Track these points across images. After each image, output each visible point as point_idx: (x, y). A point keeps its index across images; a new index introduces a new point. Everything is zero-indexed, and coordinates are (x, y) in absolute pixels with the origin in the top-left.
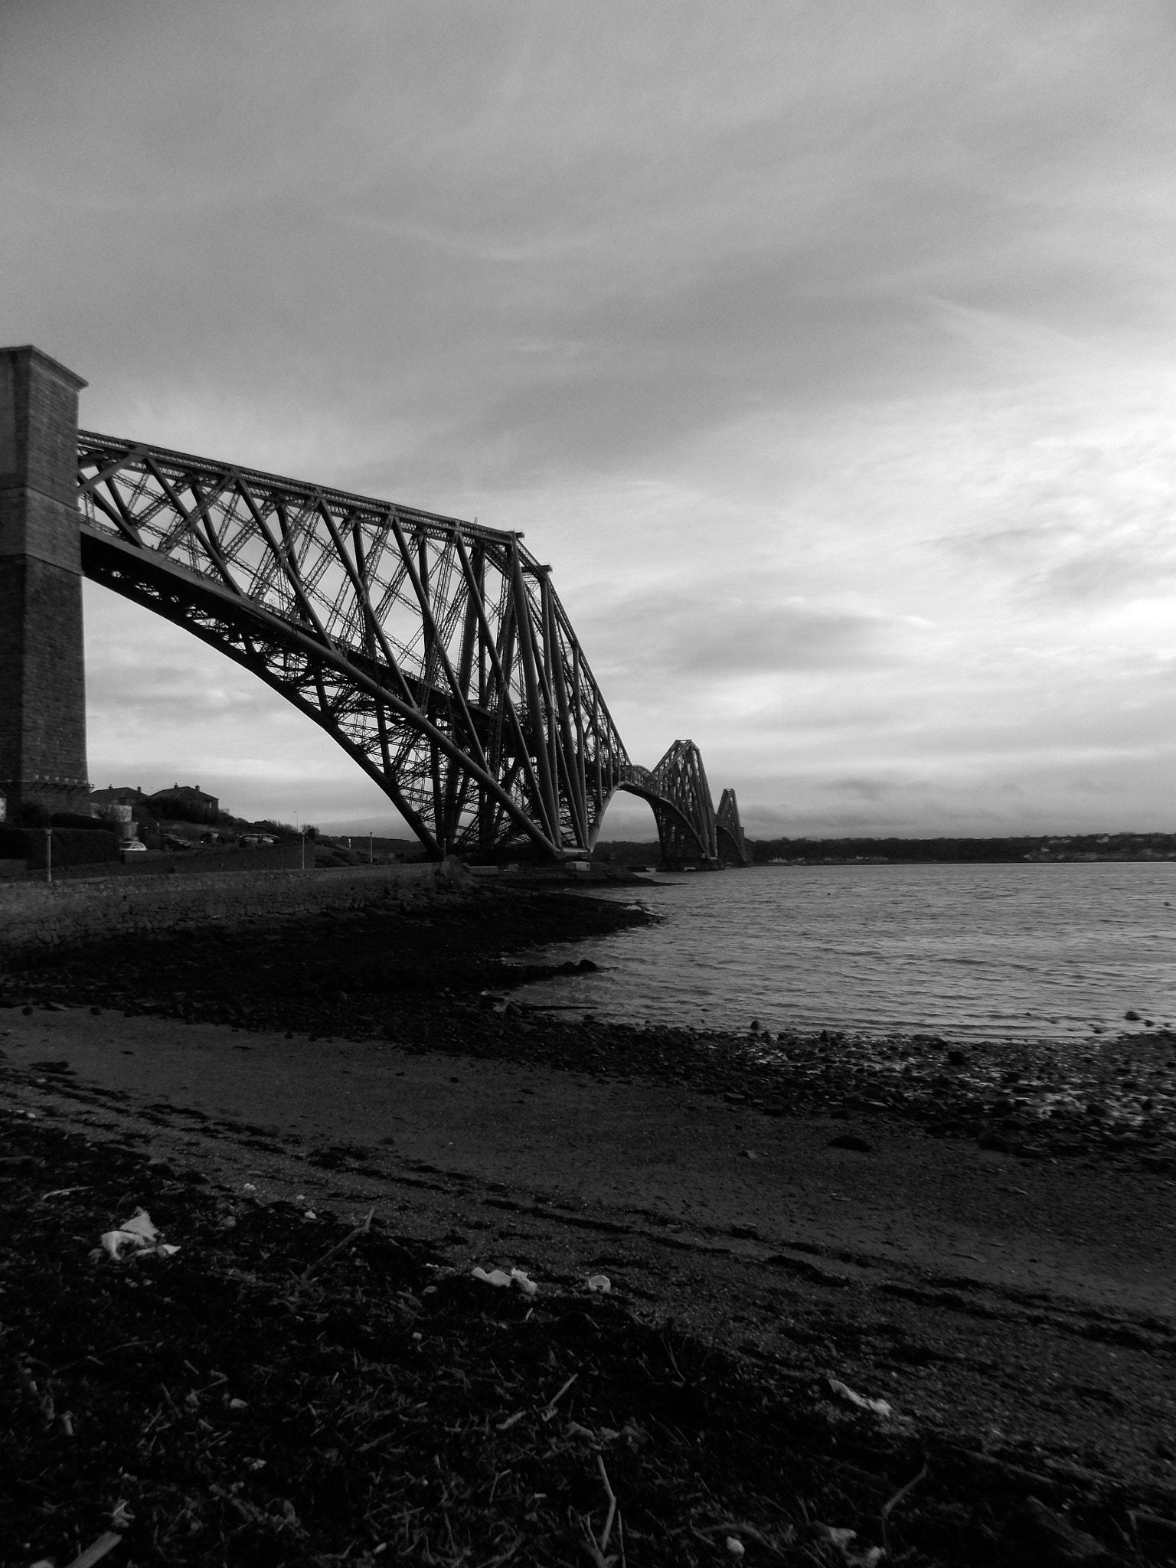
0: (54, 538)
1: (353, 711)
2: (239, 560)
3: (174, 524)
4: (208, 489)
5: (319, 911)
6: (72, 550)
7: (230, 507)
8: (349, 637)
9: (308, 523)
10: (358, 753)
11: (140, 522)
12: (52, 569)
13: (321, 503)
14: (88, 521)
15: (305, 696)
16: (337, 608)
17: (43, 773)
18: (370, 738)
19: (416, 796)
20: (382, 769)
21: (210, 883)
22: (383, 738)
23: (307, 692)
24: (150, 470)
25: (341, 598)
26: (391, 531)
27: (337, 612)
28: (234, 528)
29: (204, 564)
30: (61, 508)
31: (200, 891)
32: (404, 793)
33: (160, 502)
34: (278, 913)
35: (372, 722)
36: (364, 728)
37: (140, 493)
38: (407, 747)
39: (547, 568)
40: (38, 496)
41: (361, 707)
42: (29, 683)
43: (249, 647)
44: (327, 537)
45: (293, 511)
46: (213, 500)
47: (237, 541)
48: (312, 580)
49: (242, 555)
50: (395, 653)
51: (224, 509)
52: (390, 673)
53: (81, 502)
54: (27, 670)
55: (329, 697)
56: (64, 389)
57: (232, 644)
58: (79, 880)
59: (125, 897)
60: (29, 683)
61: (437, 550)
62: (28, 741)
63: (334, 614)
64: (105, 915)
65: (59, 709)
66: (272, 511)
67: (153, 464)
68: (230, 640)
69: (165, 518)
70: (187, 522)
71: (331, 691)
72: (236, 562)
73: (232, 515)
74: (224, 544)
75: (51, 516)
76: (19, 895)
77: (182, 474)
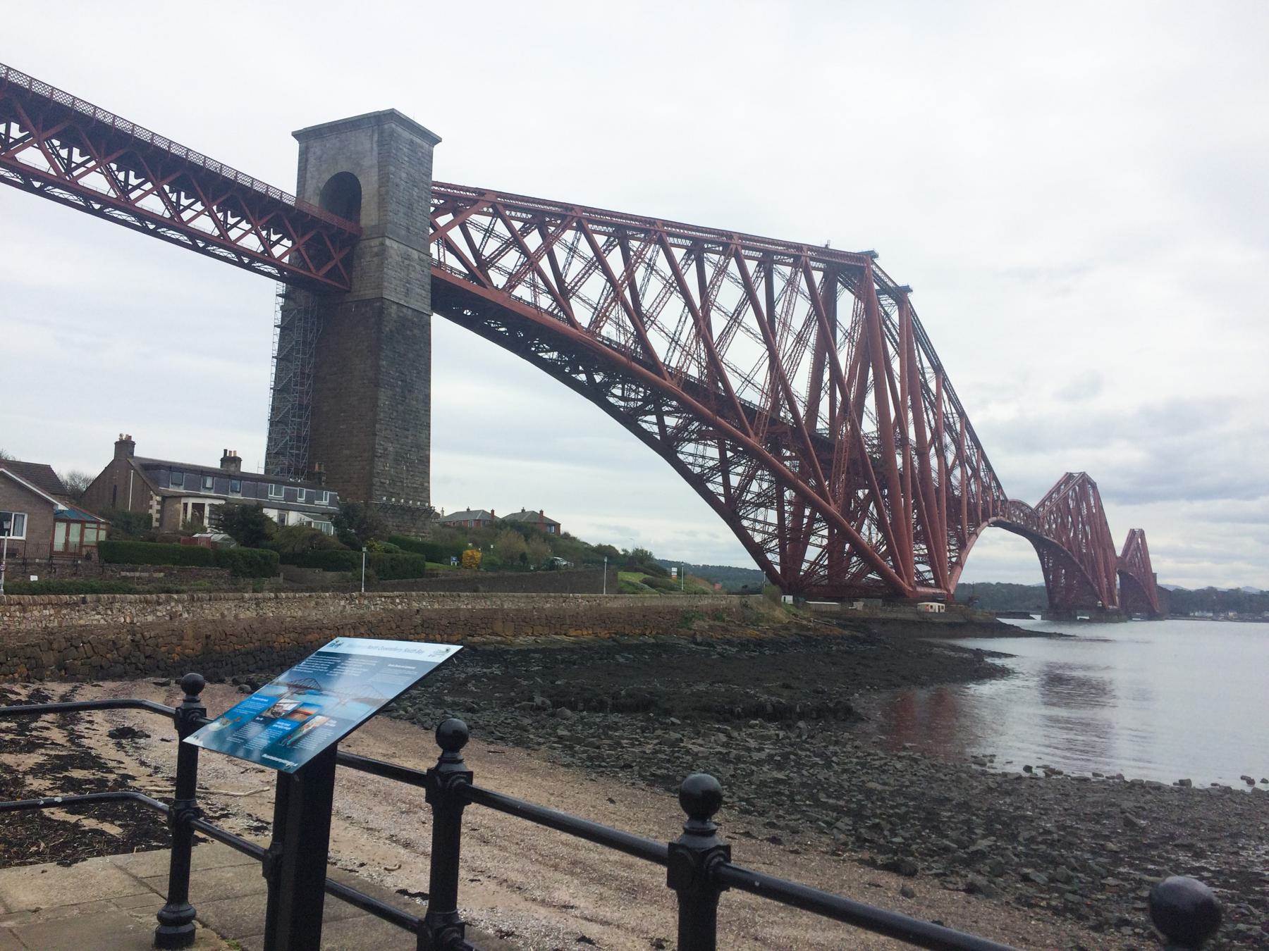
1: (690, 441)
3: (519, 263)
4: (553, 229)
5: (608, 635)
8: (685, 367)
9: (648, 256)
10: (698, 482)
12: (405, 310)
13: (661, 236)
14: (440, 265)
15: (644, 425)
16: (676, 338)
17: (391, 495)
18: (709, 468)
19: (758, 526)
20: (722, 499)
21: (499, 603)
22: (724, 467)
23: (646, 422)
24: (497, 214)
25: (680, 328)
26: (733, 260)
27: (676, 343)
28: (577, 266)
29: (545, 302)
30: (415, 255)
31: (489, 609)
32: (745, 523)
33: (507, 246)
34: (565, 634)
35: (713, 452)
36: (703, 457)
37: (489, 237)
38: (748, 478)
39: (907, 290)
40: (395, 245)
41: (701, 437)
42: (382, 414)
44: (668, 272)
45: (634, 244)
46: (557, 238)
47: (580, 276)
49: (584, 291)
50: (735, 383)
51: (566, 246)
52: (727, 403)
53: (433, 248)
54: (380, 403)
55: (668, 426)
56: (422, 147)
57: (574, 376)
58: (376, 594)
59: (418, 611)
60: (382, 414)
61: (783, 276)
62: (379, 466)
63: (674, 344)
64: (398, 627)
65: (407, 438)
66: (615, 246)
67: (500, 208)
68: (571, 372)
69: (512, 260)
70: (531, 262)
71: (671, 421)
72: (580, 298)
73: (575, 252)
74: (568, 280)
76: (317, 604)
77: (530, 216)
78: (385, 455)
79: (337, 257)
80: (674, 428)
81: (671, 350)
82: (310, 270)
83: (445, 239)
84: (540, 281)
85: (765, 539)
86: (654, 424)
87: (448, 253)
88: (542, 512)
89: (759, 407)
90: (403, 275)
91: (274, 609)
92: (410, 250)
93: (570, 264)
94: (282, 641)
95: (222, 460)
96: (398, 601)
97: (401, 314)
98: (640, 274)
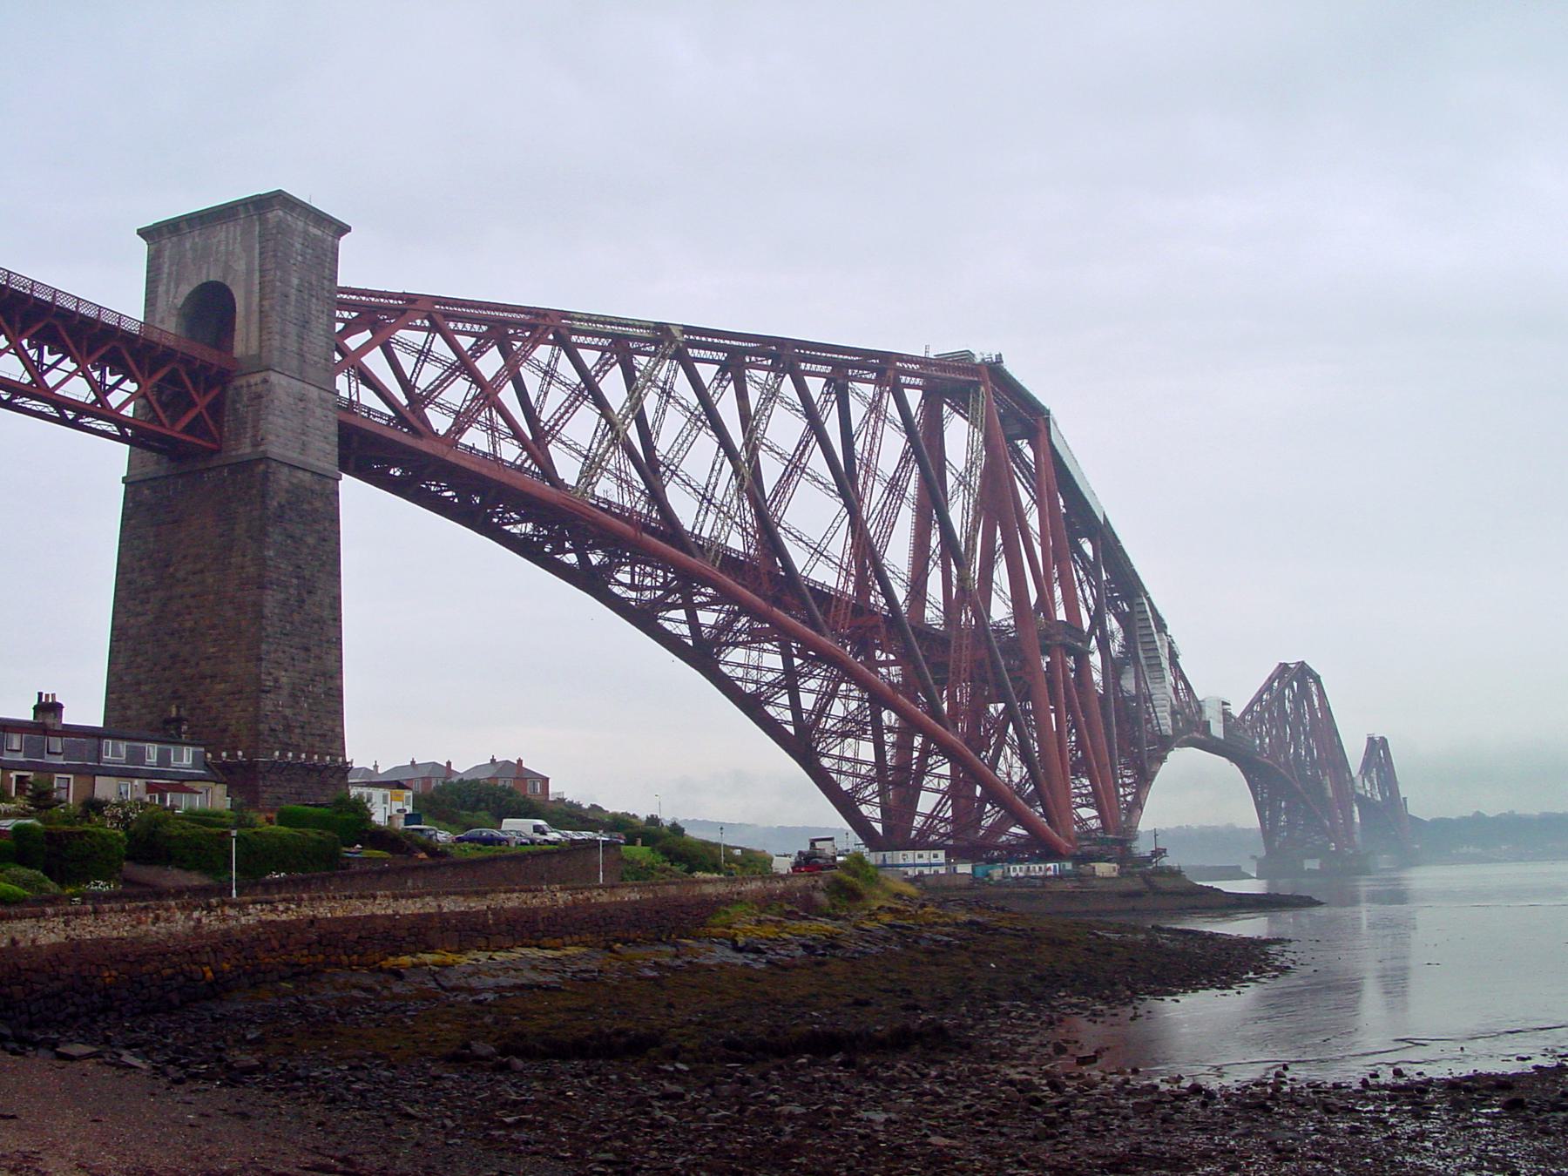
0: (304, 434)
1: (736, 645)
2: (564, 439)
3: (469, 397)
4: (519, 344)
6: (327, 446)
7: (549, 365)
8: (722, 537)
9: (662, 376)
10: (752, 706)
11: (429, 397)
12: (300, 474)
14: (352, 406)
15: (667, 625)
16: (708, 495)
18: (767, 684)
19: (846, 767)
20: (791, 729)
22: (790, 682)
23: (669, 619)
24: (435, 328)
25: (713, 480)
26: (788, 376)
27: (709, 501)
29: (510, 451)
32: (826, 762)
33: (452, 372)
35: (774, 661)
37: (424, 361)
38: (827, 697)
40: (284, 381)
41: (755, 639)
43: (583, 559)
44: (694, 400)
45: (641, 361)
47: (562, 410)
48: (675, 457)
49: (567, 432)
50: (799, 557)
51: (541, 369)
53: (342, 383)
54: (267, 611)
57: (558, 556)
61: (863, 398)
63: (705, 505)
64: (283, 946)
66: (612, 365)
67: (438, 318)
68: (553, 552)
69: (459, 392)
70: (487, 394)
71: (707, 618)
72: (562, 442)
73: (552, 376)
74: (544, 417)
75: (302, 405)
77: (484, 328)
78: (277, 687)
79: (202, 402)
80: (712, 627)
81: (703, 512)
82: (163, 425)
83: (359, 368)
84: (501, 421)
85: (856, 786)
86: (681, 622)
87: (361, 387)
88: (520, 761)
89: (836, 590)
91: (91, 929)
92: (306, 386)
93: (546, 394)
94: (106, 974)
95: (35, 708)
96: (281, 908)
97: (295, 481)
98: (651, 402)
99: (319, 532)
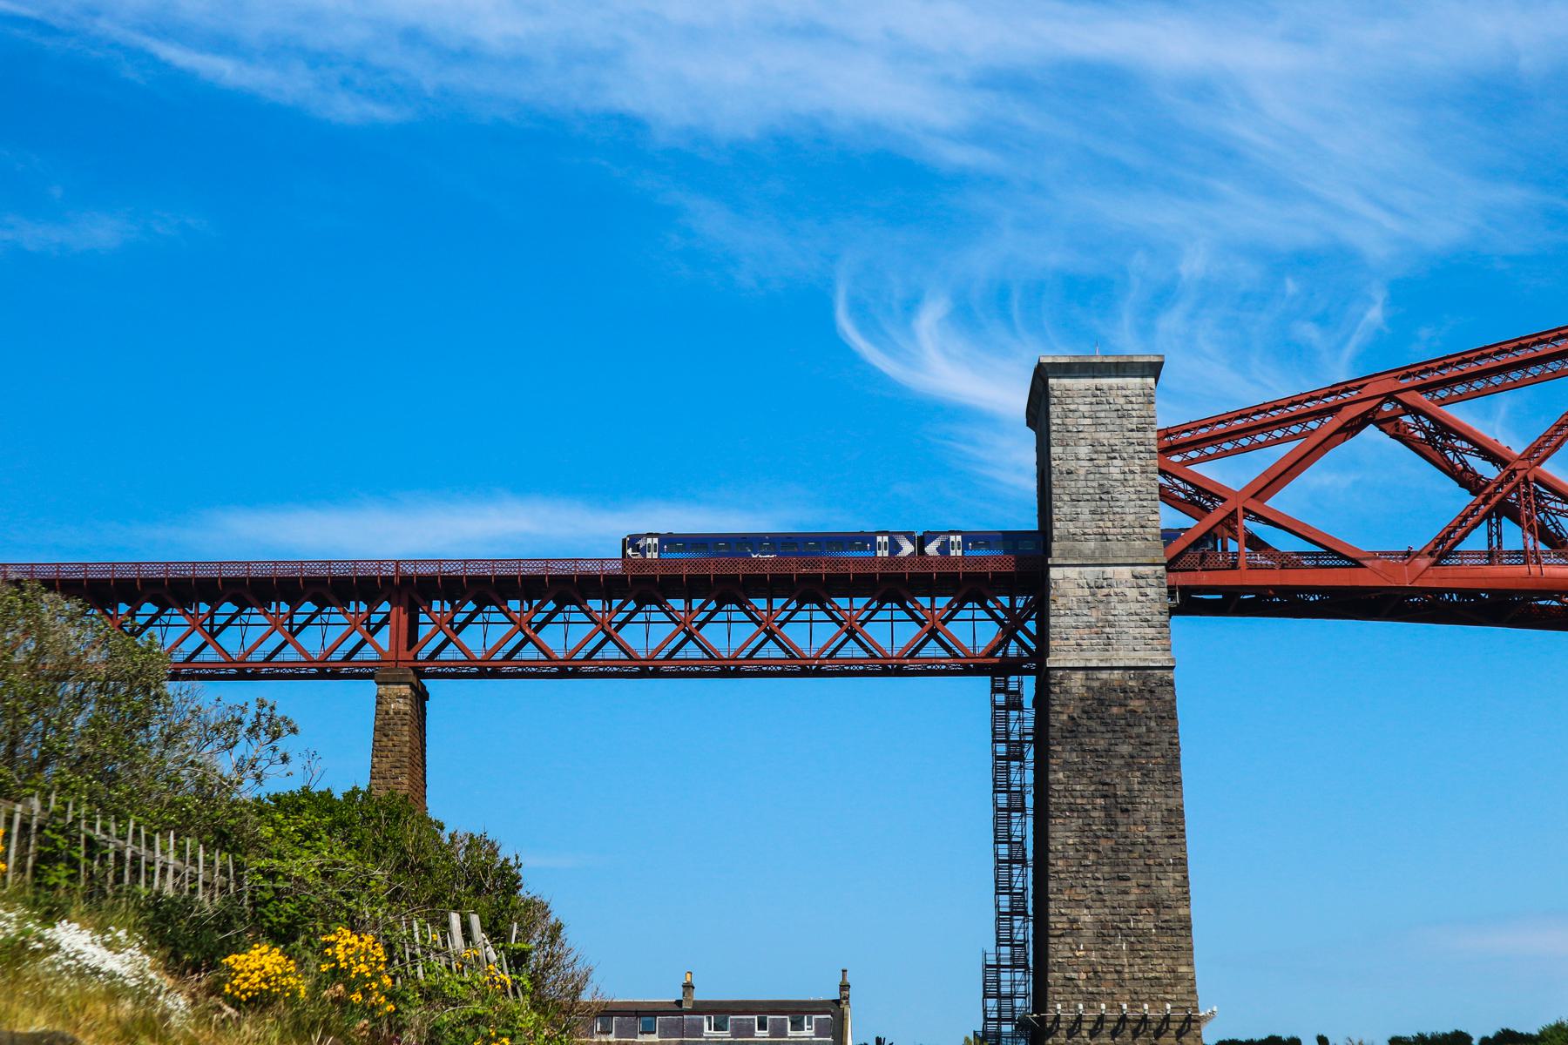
12: (1104, 675)
40: (1072, 572)
78: (1074, 928)
90: (1093, 617)
99: (1139, 736)
